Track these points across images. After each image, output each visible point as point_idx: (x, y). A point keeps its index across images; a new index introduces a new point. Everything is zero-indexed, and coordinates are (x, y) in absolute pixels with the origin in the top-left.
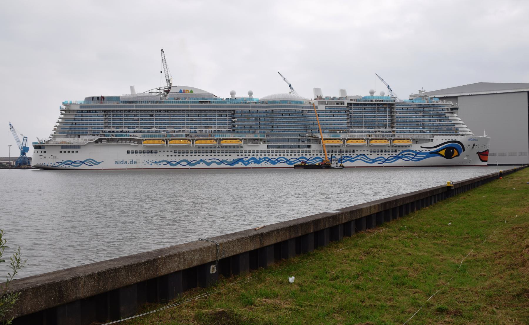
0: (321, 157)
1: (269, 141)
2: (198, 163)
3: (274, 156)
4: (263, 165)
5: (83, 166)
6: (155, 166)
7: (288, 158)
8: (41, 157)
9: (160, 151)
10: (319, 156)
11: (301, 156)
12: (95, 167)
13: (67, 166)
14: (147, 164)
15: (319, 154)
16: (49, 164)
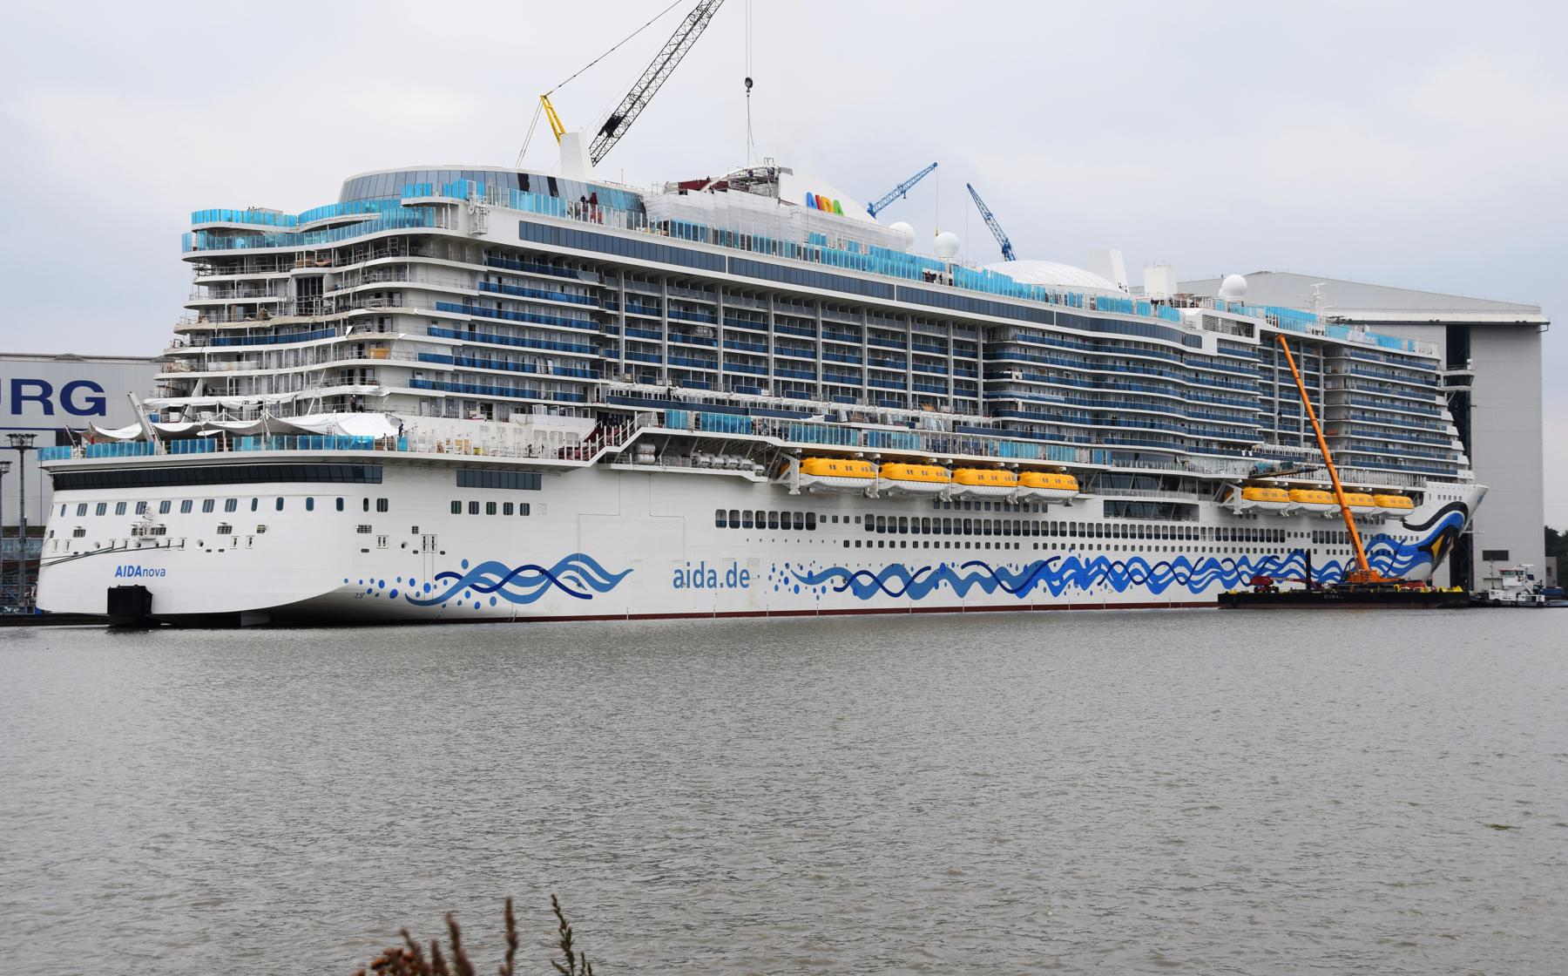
0: (1219, 557)
1: (1112, 480)
2: (933, 583)
3: (1118, 552)
4: (1101, 593)
5: (554, 602)
6: (807, 599)
7: (1152, 559)
8: (368, 540)
9: (823, 519)
10: (1215, 555)
11: (1177, 554)
12: (601, 603)
13: (484, 599)
14: (782, 585)
15: (1215, 544)
16: (404, 589)
